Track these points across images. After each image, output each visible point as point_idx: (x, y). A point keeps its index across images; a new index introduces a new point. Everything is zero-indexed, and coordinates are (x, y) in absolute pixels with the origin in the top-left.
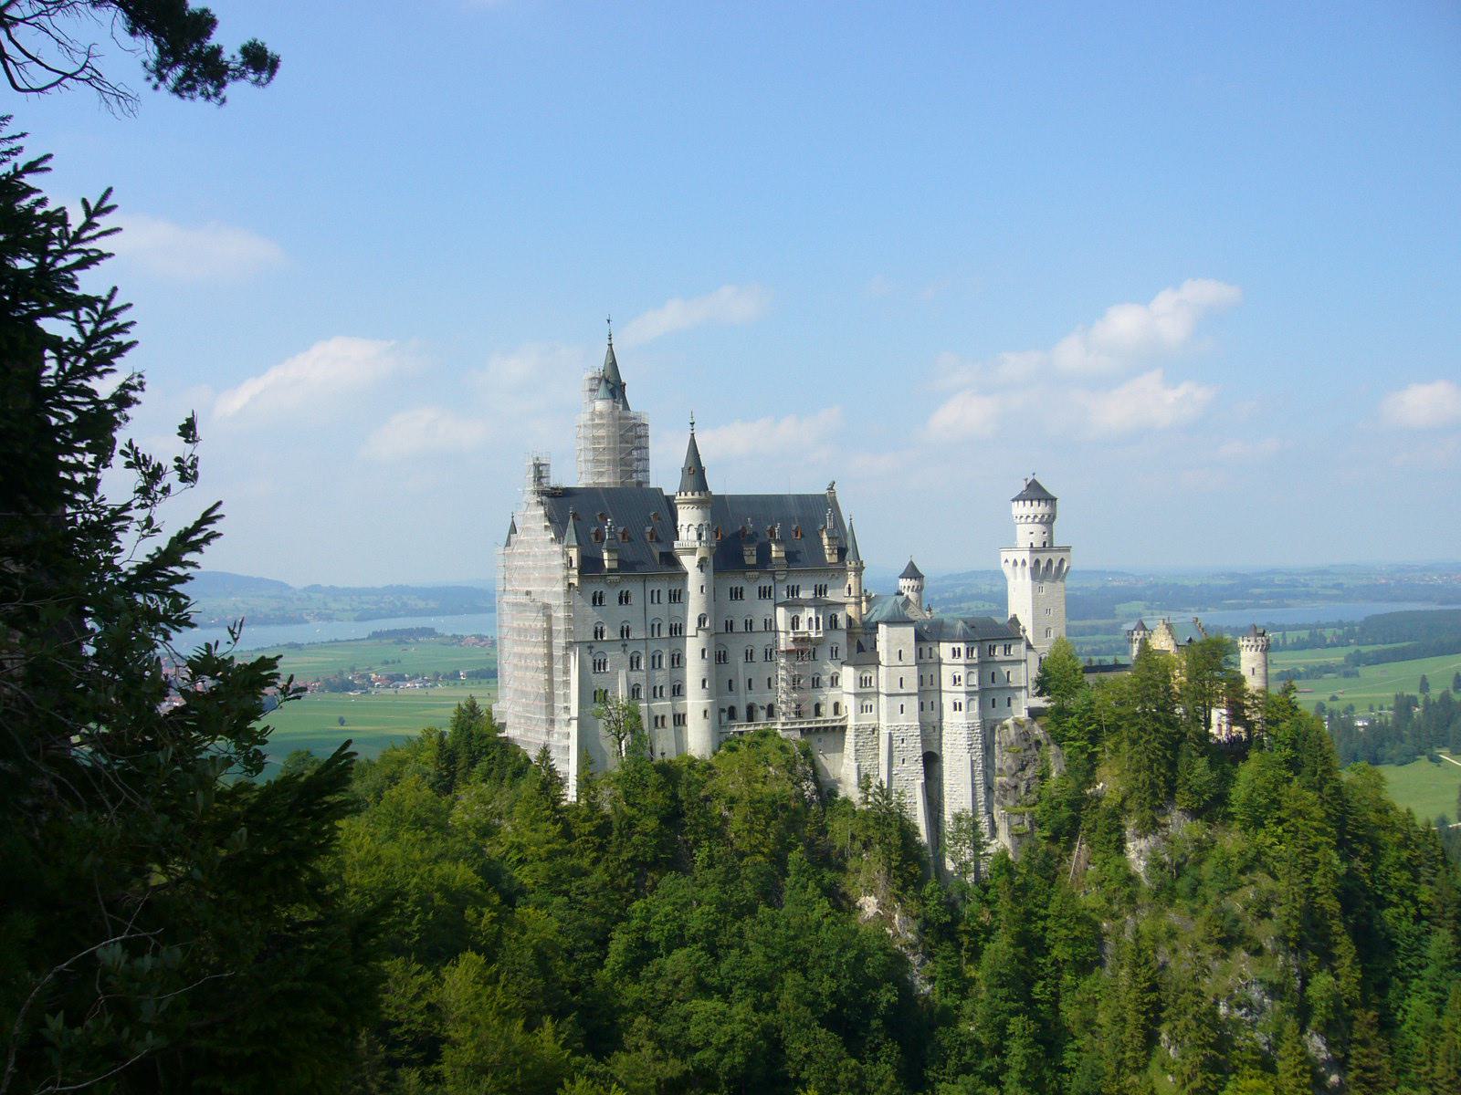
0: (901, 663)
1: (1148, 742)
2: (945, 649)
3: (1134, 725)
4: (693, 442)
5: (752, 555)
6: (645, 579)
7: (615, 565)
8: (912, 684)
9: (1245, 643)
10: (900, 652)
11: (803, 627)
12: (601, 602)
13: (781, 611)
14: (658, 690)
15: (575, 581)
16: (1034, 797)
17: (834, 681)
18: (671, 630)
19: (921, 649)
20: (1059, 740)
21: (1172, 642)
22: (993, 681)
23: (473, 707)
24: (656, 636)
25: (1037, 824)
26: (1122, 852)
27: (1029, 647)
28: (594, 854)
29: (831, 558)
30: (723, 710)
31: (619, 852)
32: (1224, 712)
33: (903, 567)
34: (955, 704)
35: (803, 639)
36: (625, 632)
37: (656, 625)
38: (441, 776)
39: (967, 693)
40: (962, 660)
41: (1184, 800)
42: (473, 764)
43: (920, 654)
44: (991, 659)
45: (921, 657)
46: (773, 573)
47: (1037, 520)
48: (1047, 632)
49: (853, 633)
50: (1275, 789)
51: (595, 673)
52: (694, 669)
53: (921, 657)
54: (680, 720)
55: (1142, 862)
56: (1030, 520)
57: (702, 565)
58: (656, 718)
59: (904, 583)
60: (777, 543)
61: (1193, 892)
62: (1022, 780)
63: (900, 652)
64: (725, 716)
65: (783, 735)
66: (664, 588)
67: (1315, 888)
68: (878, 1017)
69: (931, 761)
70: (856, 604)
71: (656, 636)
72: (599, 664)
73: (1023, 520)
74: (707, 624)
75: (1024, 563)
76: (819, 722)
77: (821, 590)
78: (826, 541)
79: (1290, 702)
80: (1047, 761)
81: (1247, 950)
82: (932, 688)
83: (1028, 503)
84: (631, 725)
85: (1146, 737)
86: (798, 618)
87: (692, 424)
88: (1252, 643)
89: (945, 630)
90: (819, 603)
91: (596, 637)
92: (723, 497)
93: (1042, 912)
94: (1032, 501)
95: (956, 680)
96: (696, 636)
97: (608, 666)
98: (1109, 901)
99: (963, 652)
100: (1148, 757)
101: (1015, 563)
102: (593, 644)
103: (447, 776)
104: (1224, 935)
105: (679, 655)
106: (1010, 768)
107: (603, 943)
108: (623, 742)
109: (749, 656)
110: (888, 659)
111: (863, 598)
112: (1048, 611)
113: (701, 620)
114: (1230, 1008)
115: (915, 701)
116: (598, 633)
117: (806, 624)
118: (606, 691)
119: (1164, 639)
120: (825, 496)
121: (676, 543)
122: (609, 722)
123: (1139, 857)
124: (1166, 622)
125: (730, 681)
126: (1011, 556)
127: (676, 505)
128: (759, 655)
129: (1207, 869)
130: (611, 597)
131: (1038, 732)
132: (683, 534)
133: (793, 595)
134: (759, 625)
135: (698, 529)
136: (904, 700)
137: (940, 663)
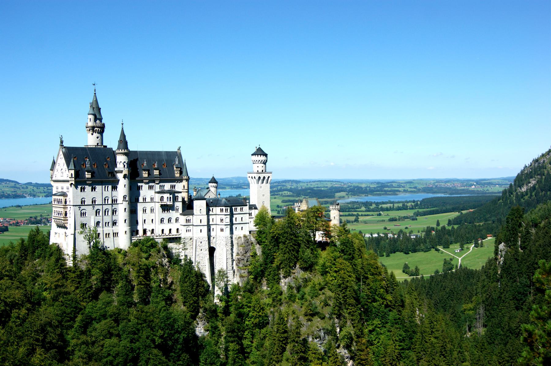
2: (217, 210)
4: (123, 131)
7: (90, 176)
8: (205, 222)
9: (332, 208)
11: (165, 200)
12: (84, 190)
13: (157, 194)
14: (107, 224)
15: (73, 182)
16: (249, 263)
17: (177, 220)
20: (259, 243)
23: (38, 230)
24: (106, 203)
25: (250, 273)
26: (279, 283)
28: (76, 285)
30: (134, 231)
31: (85, 285)
32: (322, 232)
33: (211, 178)
35: (165, 205)
36: (94, 201)
38: (22, 256)
39: (225, 225)
40: (224, 213)
42: (34, 252)
43: (208, 211)
47: (260, 162)
50: (335, 260)
52: (122, 215)
54: (116, 234)
57: (125, 177)
58: (106, 234)
59: (210, 184)
60: (156, 169)
61: (302, 298)
64: (135, 233)
65: (156, 240)
67: (347, 295)
68: (180, 344)
69: (212, 250)
71: (106, 203)
77: (173, 187)
78: (175, 169)
79: (345, 229)
81: (320, 317)
83: (257, 156)
84: (93, 237)
85: (288, 241)
86: (163, 197)
87: (122, 124)
88: (334, 208)
89: (219, 202)
91: (82, 203)
93: (249, 305)
94: (258, 155)
95: (222, 220)
98: (273, 300)
99: (224, 210)
101: (252, 177)
103: (24, 256)
104: (311, 312)
105: (116, 211)
106: (241, 252)
107: (73, 319)
108: (92, 243)
109: (144, 211)
113: (124, 197)
114: (313, 338)
116: (83, 202)
118: (86, 224)
119: (305, 206)
120: (176, 152)
122: (85, 236)
126: (251, 175)
128: (148, 211)
129: (307, 290)
130: (88, 188)
131: (253, 239)
134: (148, 200)
136: (201, 228)
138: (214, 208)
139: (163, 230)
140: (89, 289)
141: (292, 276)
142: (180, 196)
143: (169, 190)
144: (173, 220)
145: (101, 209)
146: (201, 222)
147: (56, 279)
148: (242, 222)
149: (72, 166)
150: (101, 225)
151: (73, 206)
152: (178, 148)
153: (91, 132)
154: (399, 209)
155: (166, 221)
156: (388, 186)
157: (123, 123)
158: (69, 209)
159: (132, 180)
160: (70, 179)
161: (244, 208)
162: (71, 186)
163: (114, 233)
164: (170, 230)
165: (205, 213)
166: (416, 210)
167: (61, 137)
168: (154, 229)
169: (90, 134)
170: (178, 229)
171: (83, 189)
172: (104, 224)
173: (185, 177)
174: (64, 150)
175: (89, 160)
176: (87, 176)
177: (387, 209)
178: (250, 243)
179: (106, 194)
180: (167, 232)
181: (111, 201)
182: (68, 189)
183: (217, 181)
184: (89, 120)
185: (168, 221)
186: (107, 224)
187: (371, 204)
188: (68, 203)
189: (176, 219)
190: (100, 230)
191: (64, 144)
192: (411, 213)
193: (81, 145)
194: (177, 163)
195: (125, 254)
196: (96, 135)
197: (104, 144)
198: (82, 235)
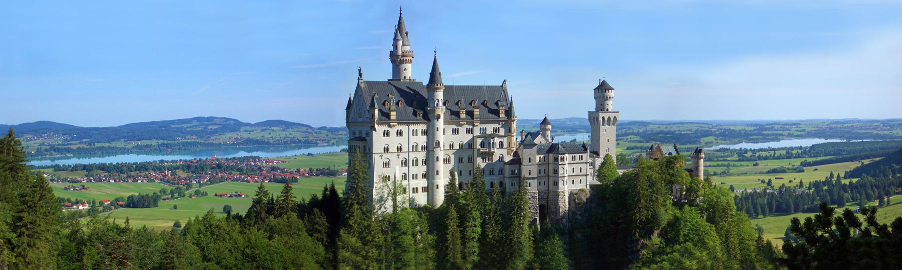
0: (530, 164)
6: (408, 124)
8: (535, 174)
19: (540, 157)
29: (502, 115)
34: (554, 182)
36: (400, 149)
37: (415, 145)
44: (572, 162)
48: (608, 150)
51: (383, 167)
58: (413, 189)
72: (386, 164)
82: (544, 175)
83: (600, 90)
86: (484, 143)
91: (385, 151)
92: (452, 87)
101: (594, 117)
102: (382, 154)
112: (608, 140)
115: (536, 180)
116: (387, 150)
118: (389, 176)
128: (465, 160)
130: (393, 132)
142: (505, 140)
143: (491, 135)
148: (581, 174)
154: (779, 158)
156: (766, 129)
160: (369, 120)
161: (584, 155)
163: (423, 188)
166: (803, 160)
172: (411, 177)
177: (766, 158)
179: (414, 140)
181: (421, 148)
186: (415, 177)
187: (746, 151)
189: (499, 170)
190: (405, 183)
192: (797, 162)
194: (502, 100)
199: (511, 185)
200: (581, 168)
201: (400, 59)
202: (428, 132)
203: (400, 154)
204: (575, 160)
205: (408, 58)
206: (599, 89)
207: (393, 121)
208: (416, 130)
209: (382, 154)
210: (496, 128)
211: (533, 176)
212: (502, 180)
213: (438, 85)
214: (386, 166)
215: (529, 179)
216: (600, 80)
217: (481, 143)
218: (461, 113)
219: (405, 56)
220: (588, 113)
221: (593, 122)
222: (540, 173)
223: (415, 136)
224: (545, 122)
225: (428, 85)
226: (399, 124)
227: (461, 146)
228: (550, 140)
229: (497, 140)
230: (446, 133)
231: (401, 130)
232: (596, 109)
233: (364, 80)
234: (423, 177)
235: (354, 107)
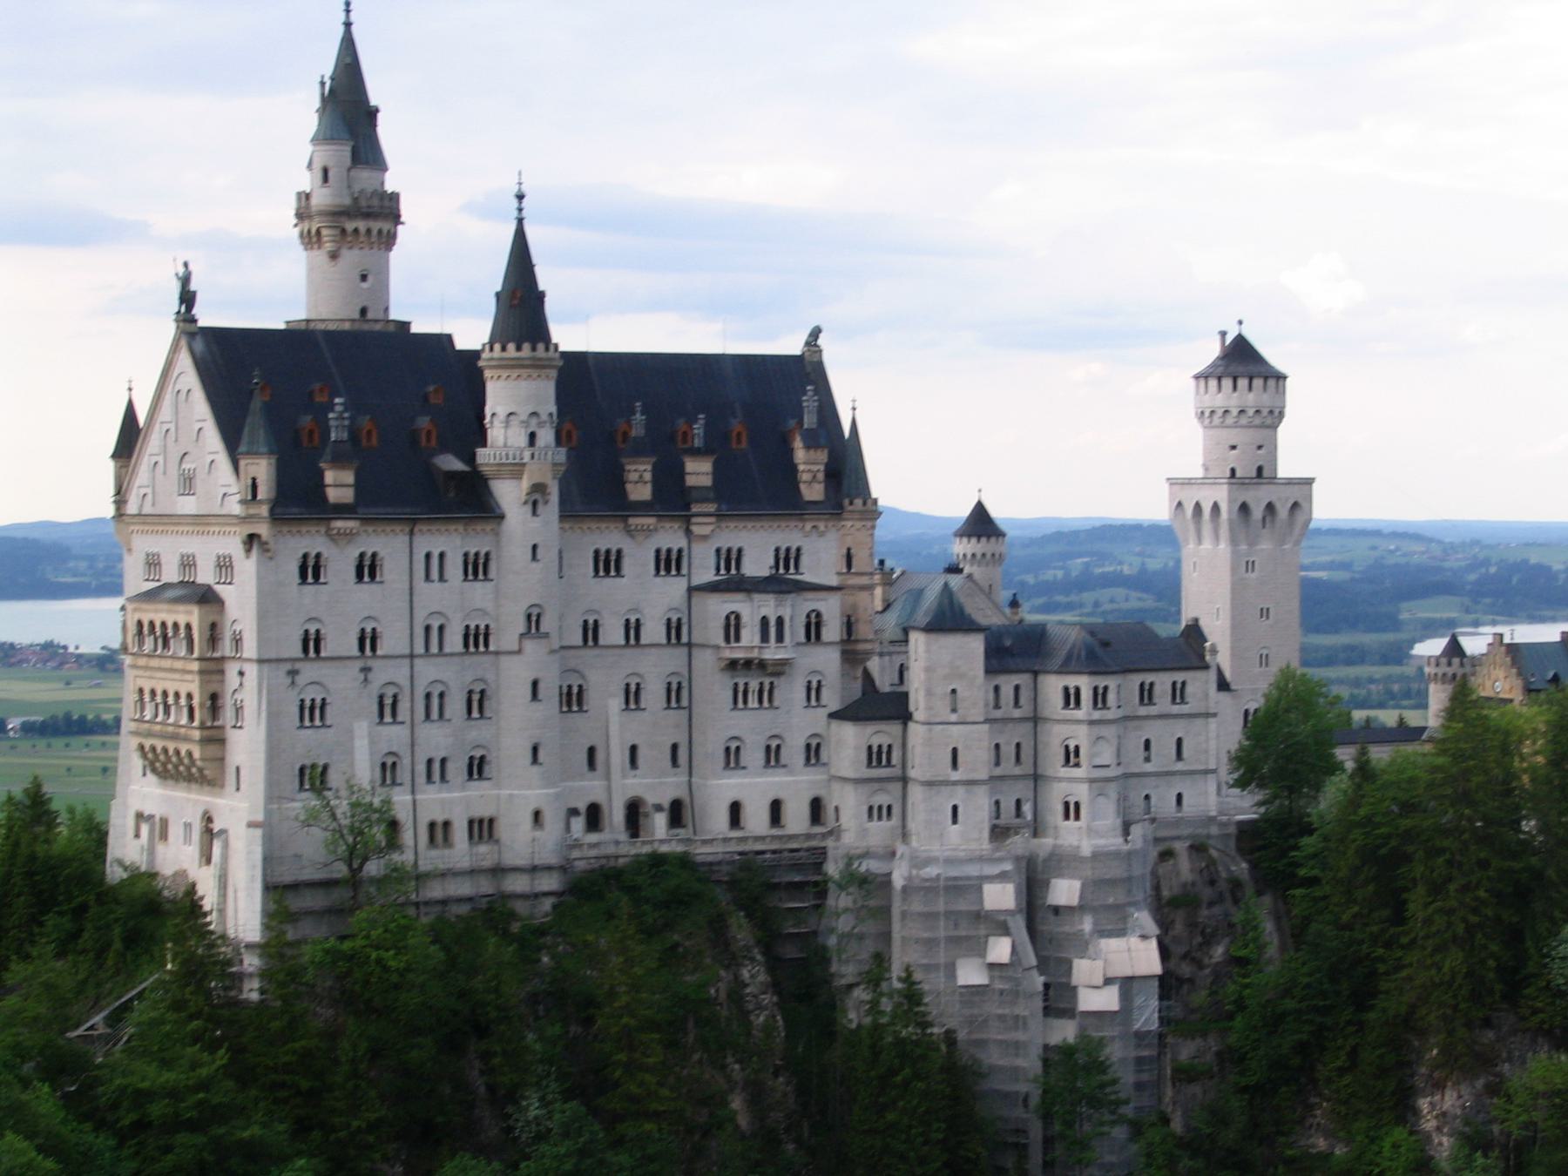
0: (954, 718)
1: (1465, 888)
3: (1441, 851)
5: (641, 480)
8: (977, 762)
10: (954, 691)
11: (750, 636)
12: (317, 576)
14: (436, 766)
15: (263, 530)
17: (813, 753)
18: (466, 636)
19: (997, 689)
21: (1518, 683)
22: (1147, 759)
24: (434, 649)
27: (1223, 685)
29: (813, 491)
33: (964, 511)
34: (1067, 805)
35: (748, 663)
36: (368, 641)
37: (435, 625)
39: (1092, 781)
41: (1535, 1012)
45: (997, 706)
46: (687, 520)
48: (1264, 660)
49: (855, 652)
53: (997, 706)
54: (482, 829)
55: (1445, 1140)
56: (1230, 420)
58: (432, 825)
62: (1201, 966)
63: (954, 691)
64: (578, 824)
66: (452, 542)
70: (863, 588)
71: (434, 649)
72: (312, 709)
73: (1217, 420)
74: (542, 629)
75: (1216, 508)
76: (780, 838)
77: (788, 558)
78: (800, 454)
80: (1255, 928)
82: (1017, 771)
83: (1227, 383)
86: (738, 617)
87: (520, 197)
90: (783, 581)
91: (306, 650)
96: (519, 652)
97: (328, 709)
99: (1086, 696)
100: (1464, 920)
105: (482, 692)
109: (633, 696)
110: (929, 708)
111: (877, 578)
112: (1264, 613)
113: (533, 621)
116: (312, 643)
117: (757, 629)
118: (325, 768)
120: (797, 360)
121: (480, 452)
123: (1439, 1129)
124: (1507, 640)
125: (591, 751)
127: (480, 372)
128: (653, 695)
130: (340, 563)
131: (1241, 868)
132: (496, 433)
133: (728, 569)
134: (654, 631)
135: (525, 423)
136: (959, 796)
137: (1036, 720)
138: (1023, 679)
139: (735, 809)
140: (371, 1139)
141: (1480, 1083)
142: (831, 608)
143: (766, 579)
144: (794, 752)
145: (405, 683)
146: (955, 764)
147: (204, 1072)
148: (1180, 766)
149: (255, 426)
150: (404, 774)
151: (260, 661)
152: (803, 337)
153: (328, 246)
155: (753, 755)
157: (525, 188)
158: (232, 679)
159: (567, 526)
160: (237, 509)
162: (248, 550)
163: (471, 822)
164: (776, 808)
165: (977, 713)
167: (181, 270)
168: (687, 800)
169: (320, 256)
170: (816, 807)
171: (311, 570)
172: (421, 768)
173: (858, 502)
174: (199, 345)
175: (346, 407)
176: (333, 495)
178: (1223, 886)
179: (433, 597)
180: (756, 821)
182: (224, 566)
183: (1003, 526)
184: (319, 175)
185: (760, 755)
186: (437, 770)
188: (226, 648)
189: (808, 746)
190: (401, 799)
191: (195, 311)
193: (275, 321)
194: (809, 420)
195: (531, 940)
196: (352, 258)
197: (396, 314)
198: (315, 831)
199: (866, 816)
200: (1179, 742)
201: (343, 231)
202: (493, 566)
203: (375, 664)
204: (1151, 702)
205: (376, 226)
206: (1219, 379)
207: (342, 510)
208: (442, 556)
209: (298, 666)
210: (788, 550)
211: (965, 777)
212: (822, 793)
213: (534, 349)
214: (312, 719)
215: (955, 783)
216: (1223, 334)
217: (728, 618)
218: (633, 476)
219: (368, 215)
220: (1166, 486)
221: (1192, 527)
222: (997, 764)
223: (437, 585)
224: (980, 523)
225: (491, 344)
226: (366, 521)
227: (633, 630)
228: (1008, 611)
229: (794, 610)
230: (565, 568)
231: (374, 555)
232: (1206, 469)
233: (201, 323)
234: (470, 773)
235: (151, 448)
